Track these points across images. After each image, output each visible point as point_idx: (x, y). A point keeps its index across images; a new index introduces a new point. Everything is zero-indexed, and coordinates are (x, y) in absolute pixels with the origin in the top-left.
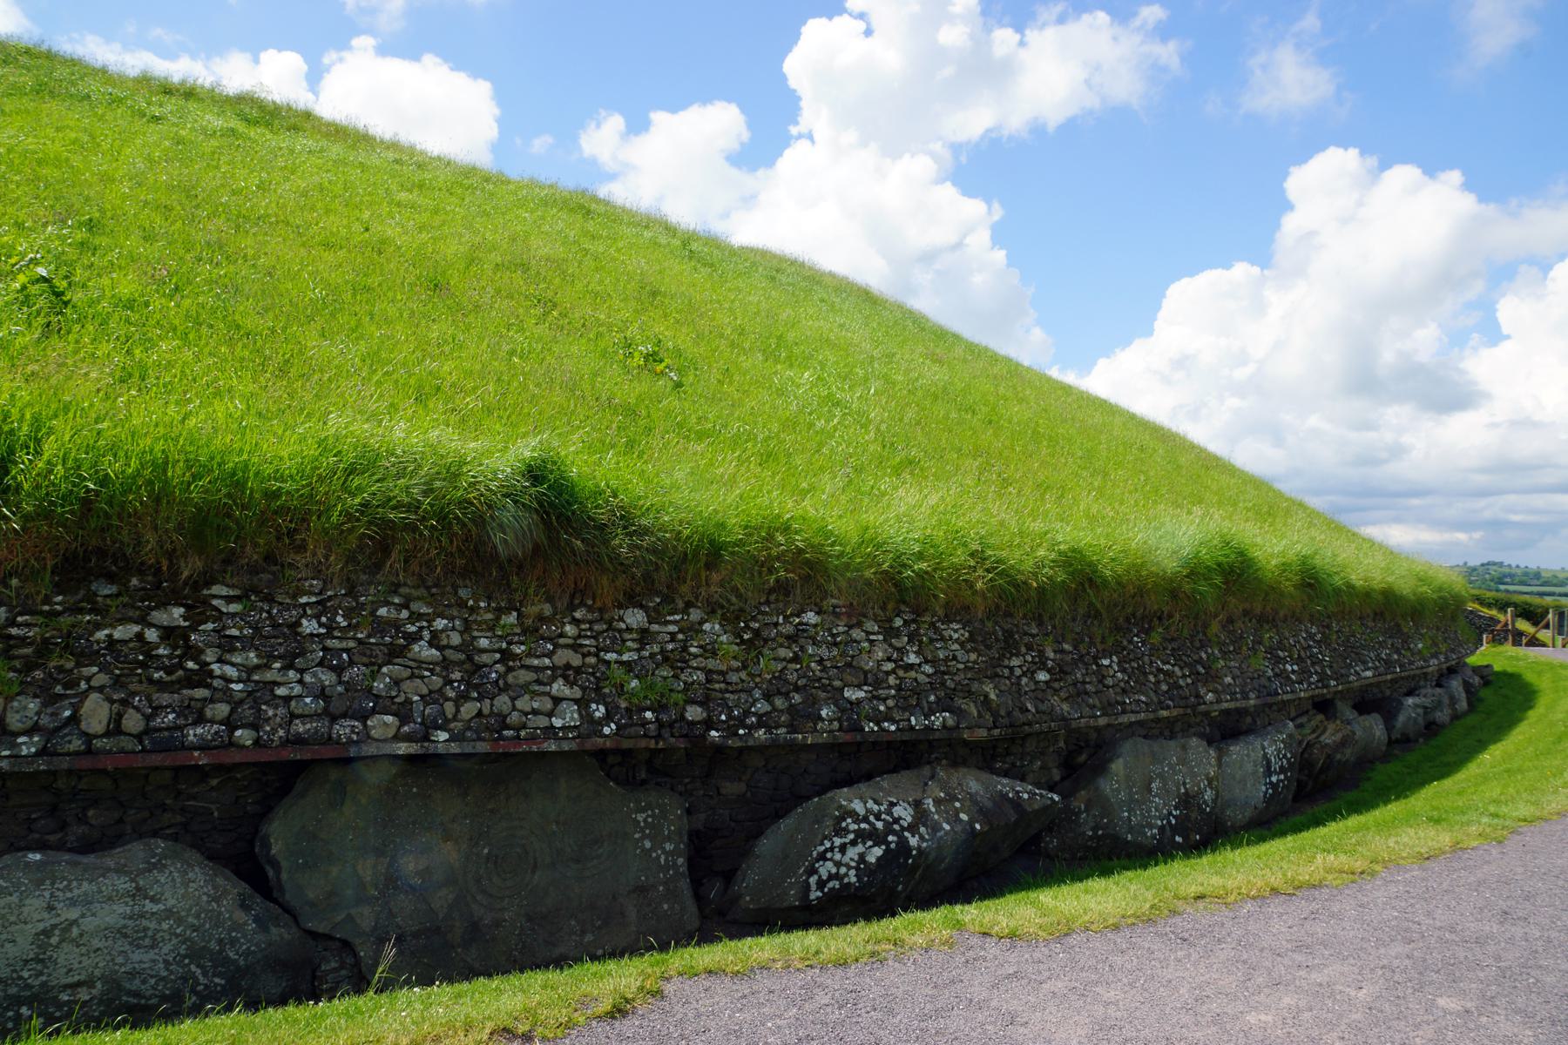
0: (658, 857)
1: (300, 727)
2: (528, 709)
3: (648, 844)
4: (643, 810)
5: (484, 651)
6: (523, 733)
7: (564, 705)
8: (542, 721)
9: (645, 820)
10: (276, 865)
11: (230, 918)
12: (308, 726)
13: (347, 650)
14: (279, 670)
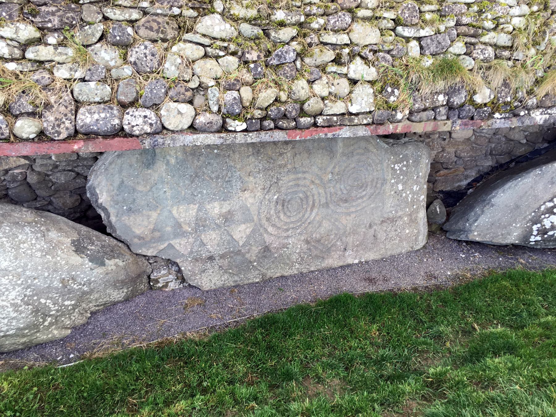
0: (407, 197)
1: (87, 118)
2: (325, 93)
3: (400, 187)
5: (282, 24)
6: (320, 120)
7: (358, 89)
8: (339, 108)
9: (401, 169)
10: (105, 209)
11: (67, 263)
12: (96, 116)
13: (132, 22)
14: (56, 47)
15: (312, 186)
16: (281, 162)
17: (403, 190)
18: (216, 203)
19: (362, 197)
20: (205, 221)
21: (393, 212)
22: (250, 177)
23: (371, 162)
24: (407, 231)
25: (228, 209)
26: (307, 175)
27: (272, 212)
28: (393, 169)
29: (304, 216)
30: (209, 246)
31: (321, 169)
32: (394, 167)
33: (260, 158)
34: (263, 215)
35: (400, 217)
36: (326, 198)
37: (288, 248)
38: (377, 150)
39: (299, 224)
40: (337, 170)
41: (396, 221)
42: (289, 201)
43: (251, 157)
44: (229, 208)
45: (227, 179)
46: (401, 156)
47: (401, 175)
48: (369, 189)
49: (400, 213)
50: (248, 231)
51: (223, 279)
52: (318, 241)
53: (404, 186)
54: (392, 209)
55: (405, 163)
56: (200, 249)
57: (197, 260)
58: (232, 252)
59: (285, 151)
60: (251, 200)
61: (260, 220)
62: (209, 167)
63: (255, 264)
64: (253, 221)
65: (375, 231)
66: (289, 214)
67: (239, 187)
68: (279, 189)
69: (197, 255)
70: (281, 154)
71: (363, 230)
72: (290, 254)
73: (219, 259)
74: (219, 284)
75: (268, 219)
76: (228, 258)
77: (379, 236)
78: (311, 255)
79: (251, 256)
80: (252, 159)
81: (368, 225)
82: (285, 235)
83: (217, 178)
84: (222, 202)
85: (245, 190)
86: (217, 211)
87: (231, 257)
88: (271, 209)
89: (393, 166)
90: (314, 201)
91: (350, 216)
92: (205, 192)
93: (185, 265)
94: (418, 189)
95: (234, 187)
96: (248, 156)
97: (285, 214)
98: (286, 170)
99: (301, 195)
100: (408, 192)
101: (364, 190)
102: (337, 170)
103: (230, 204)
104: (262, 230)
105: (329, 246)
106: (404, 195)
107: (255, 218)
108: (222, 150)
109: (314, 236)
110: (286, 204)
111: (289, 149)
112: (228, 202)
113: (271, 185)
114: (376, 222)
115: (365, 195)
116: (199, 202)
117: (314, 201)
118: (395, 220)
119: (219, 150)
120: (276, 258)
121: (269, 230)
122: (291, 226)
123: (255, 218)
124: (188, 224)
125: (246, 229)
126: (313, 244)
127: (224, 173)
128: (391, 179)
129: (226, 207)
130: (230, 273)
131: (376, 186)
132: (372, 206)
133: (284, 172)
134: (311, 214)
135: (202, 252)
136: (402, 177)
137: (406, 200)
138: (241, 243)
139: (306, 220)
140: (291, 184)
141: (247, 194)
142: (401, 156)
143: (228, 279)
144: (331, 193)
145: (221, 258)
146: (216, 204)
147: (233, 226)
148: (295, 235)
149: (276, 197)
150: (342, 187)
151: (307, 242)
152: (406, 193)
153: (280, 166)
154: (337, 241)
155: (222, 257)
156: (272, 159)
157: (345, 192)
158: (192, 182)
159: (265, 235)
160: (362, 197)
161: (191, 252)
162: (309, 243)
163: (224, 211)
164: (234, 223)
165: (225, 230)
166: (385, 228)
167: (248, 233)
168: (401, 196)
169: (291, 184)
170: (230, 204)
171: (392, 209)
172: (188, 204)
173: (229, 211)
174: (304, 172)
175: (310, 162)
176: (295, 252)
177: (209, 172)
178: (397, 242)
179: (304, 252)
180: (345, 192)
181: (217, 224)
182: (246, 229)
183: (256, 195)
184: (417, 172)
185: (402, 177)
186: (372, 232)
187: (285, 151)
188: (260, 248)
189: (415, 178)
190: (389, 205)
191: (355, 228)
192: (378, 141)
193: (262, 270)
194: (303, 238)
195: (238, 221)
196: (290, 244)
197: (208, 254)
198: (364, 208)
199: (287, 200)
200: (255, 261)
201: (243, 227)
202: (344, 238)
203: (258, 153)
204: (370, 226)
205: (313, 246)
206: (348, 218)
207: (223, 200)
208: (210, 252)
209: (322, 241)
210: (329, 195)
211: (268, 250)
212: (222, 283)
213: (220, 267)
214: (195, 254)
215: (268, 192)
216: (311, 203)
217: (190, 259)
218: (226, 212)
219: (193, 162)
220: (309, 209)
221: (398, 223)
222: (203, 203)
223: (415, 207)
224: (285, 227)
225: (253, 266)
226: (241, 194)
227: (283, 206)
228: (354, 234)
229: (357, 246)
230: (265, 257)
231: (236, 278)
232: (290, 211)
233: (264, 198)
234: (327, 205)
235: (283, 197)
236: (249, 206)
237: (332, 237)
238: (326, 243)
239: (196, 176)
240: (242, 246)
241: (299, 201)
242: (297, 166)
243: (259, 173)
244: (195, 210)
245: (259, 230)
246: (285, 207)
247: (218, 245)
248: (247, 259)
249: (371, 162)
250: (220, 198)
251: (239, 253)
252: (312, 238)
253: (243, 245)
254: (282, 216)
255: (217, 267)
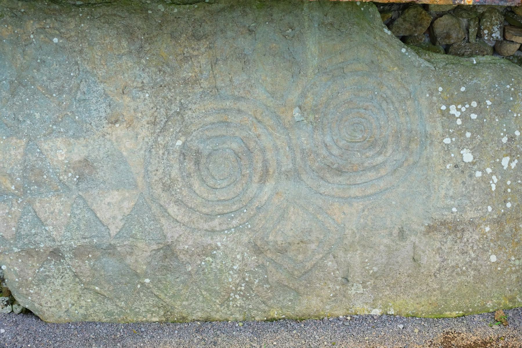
0: (486, 179)
3: (468, 157)
4: (464, 100)
9: (465, 117)
15: (260, 131)
16: (186, 73)
17: (473, 163)
18: (60, 139)
19: (375, 168)
20: (41, 173)
21: (454, 210)
22: (125, 96)
23: (389, 93)
24: (493, 258)
25: (83, 155)
26: (242, 105)
27: (175, 173)
28: (445, 114)
29: (245, 191)
30: (51, 227)
31: (273, 94)
32: (448, 109)
33: (143, 61)
34: (156, 178)
35: (471, 223)
36: (294, 159)
37: (214, 257)
38: (402, 70)
39: (234, 208)
40: (310, 101)
41: (463, 230)
42: (210, 155)
43: (124, 58)
44: (86, 153)
45: (79, 95)
46: (463, 89)
47: (467, 129)
48: (390, 151)
49: (470, 215)
50: (127, 206)
51: (83, 303)
52: (282, 251)
53: (477, 154)
54: (449, 202)
55: (474, 104)
56: (33, 231)
57: (29, 253)
58: (97, 247)
59: (195, 53)
60: (128, 144)
61: (150, 185)
62: (44, 69)
63: (147, 281)
64: (136, 186)
65: (415, 247)
66: (211, 182)
67: (104, 115)
68: (186, 127)
69: (30, 242)
70: (186, 59)
71: (386, 241)
72: (221, 271)
73: (71, 258)
74: (78, 313)
75: (167, 188)
76: (89, 259)
77: (424, 261)
78: (267, 281)
79: (136, 261)
80: (127, 62)
81: (395, 232)
82: (206, 227)
83: (60, 90)
84: (72, 140)
85: (116, 122)
86: (61, 155)
87: (97, 259)
88: (171, 166)
89: (444, 108)
90: (265, 161)
91: (351, 205)
92: (37, 115)
93: (8, 261)
94: (513, 165)
95: (94, 113)
96: (120, 56)
97: (203, 181)
98: (198, 90)
99: (234, 146)
100: (489, 170)
101: (380, 153)
102: (310, 101)
103: (87, 146)
104: (155, 208)
105: (308, 265)
106: (479, 174)
107: (140, 180)
108: (67, 39)
109: (271, 238)
110: (203, 161)
111: (203, 50)
112: (82, 141)
113: (168, 118)
114: (415, 227)
115: (384, 163)
116: (27, 135)
117: (265, 161)
118: (459, 228)
119: (62, 37)
120: (189, 274)
121: (170, 210)
122: (219, 209)
123: (140, 180)
124: (10, 175)
125: (122, 201)
126: (269, 255)
127: (74, 82)
128: (443, 136)
129: (79, 152)
130: (97, 293)
131: (407, 148)
132: (401, 189)
133: (195, 94)
134: (261, 189)
135: (38, 238)
136: (468, 135)
137: (483, 185)
138: (113, 231)
139: (251, 201)
140: (210, 119)
141: (119, 130)
142: (463, 89)
143: (94, 306)
144: (303, 151)
145: (75, 255)
146: (59, 142)
147: (95, 192)
148: (229, 229)
149: (179, 143)
150: (328, 139)
151: (258, 250)
152: (483, 171)
153: (186, 82)
154: (325, 257)
155: (79, 253)
156: (168, 65)
157: (335, 151)
158: (13, 94)
159: (163, 221)
160: (375, 168)
161: (18, 236)
162: (262, 253)
163: (76, 158)
164: (97, 185)
165: (80, 197)
166: (438, 245)
167: (127, 212)
168: (471, 176)
169: (210, 119)
170: (87, 146)
171: (449, 202)
172: (7, 137)
173: (86, 160)
174: (238, 99)
175: (248, 80)
176: (232, 269)
177: (45, 78)
178: (470, 279)
179: (250, 272)
180: (335, 151)
181: (64, 184)
182: (122, 201)
183: (137, 134)
184: (508, 128)
185: (468, 135)
186: (406, 249)
187: (195, 53)
188: (155, 247)
189: (505, 140)
190: (443, 192)
191: (365, 234)
192: (403, 50)
193: (162, 296)
194: (245, 239)
195: (104, 182)
196: (219, 248)
197: (49, 244)
198: (382, 192)
199: (206, 153)
200: (146, 276)
201: (114, 196)
202: (341, 254)
203: (139, 52)
204: (402, 235)
205: (271, 260)
206: (346, 209)
207: (74, 136)
208: (54, 240)
209: (290, 254)
210: (299, 156)
211: (173, 254)
212: (82, 311)
213: (76, 276)
214: (26, 241)
215: (163, 129)
216: (260, 165)
217: (16, 250)
218: (80, 162)
219: (13, 56)
220: (256, 179)
221: (467, 235)
222: (36, 138)
223: (509, 205)
224: (205, 210)
225: (143, 284)
226: (107, 128)
227: (197, 163)
228: (364, 246)
229: (374, 275)
230: (166, 268)
231: (110, 307)
232: (213, 178)
233: (156, 141)
234: (295, 175)
235: (195, 145)
236: (125, 154)
237: (313, 246)
238: (300, 257)
239: (20, 83)
240: (115, 238)
241: (232, 157)
242: (219, 84)
243: (142, 89)
244: (21, 150)
245: (150, 209)
246: (202, 167)
247: (68, 227)
248: (128, 266)
249: (389, 93)
250: (67, 132)
251: (110, 250)
252: (267, 243)
253: (118, 236)
254: (196, 185)
255: (68, 276)
